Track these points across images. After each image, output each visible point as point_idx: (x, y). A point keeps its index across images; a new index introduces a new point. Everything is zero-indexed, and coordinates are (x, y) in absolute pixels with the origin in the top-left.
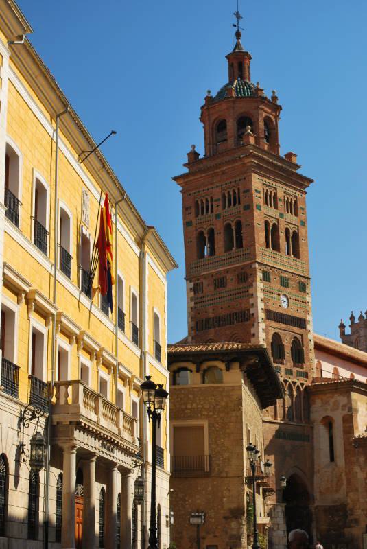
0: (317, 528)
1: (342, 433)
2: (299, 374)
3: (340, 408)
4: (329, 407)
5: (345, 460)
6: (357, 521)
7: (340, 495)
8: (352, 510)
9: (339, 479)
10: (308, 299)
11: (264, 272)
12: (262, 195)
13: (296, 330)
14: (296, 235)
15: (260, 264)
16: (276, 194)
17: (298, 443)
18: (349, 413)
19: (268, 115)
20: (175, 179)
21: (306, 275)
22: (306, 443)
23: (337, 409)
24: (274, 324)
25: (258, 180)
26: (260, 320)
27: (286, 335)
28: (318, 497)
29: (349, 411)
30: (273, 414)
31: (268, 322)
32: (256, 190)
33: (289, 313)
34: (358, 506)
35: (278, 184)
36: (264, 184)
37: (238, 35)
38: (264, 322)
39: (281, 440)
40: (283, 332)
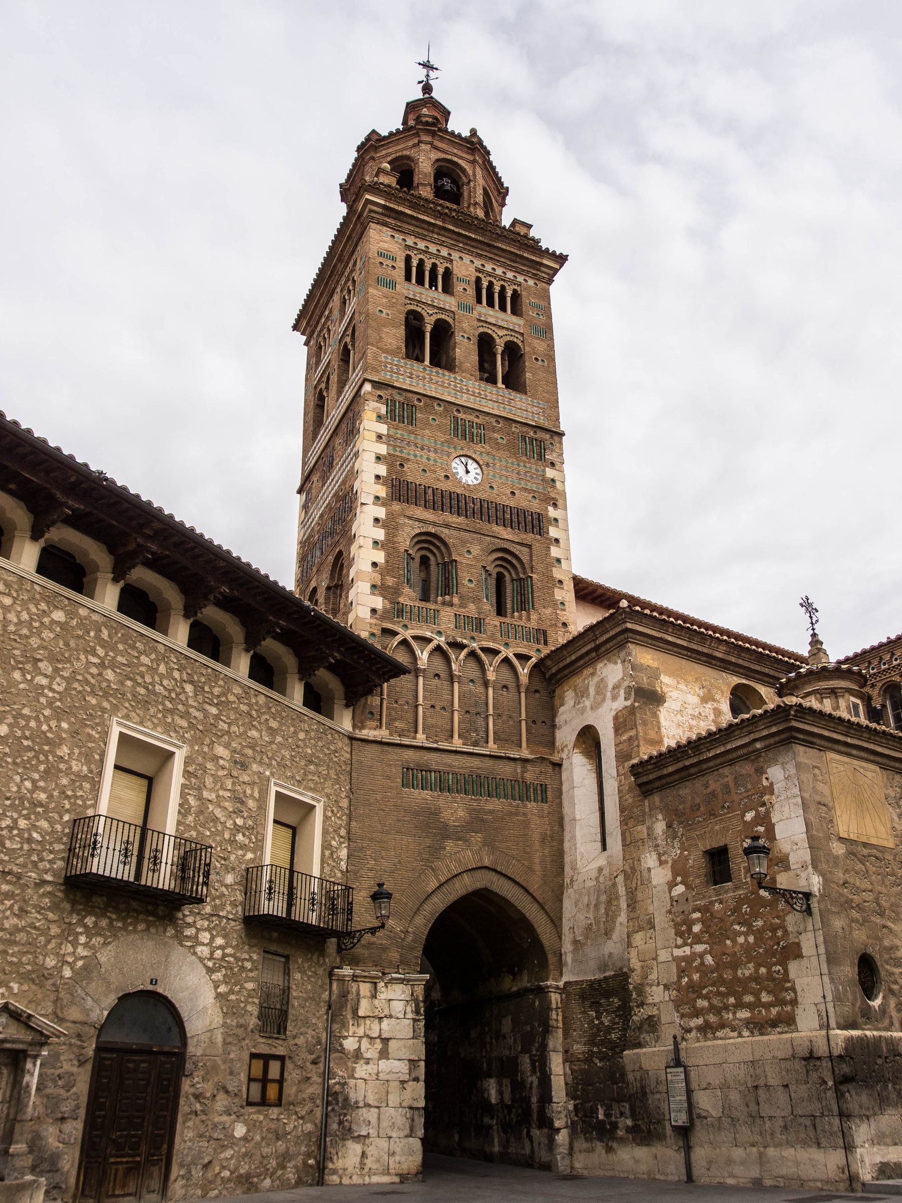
0: (566, 1051)
1: (614, 763)
2: (506, 632)
3: (609, 695)
4: (588, 703)
5: (624, 840)
6: (652, 1024)
7: (612, 946)
8: (640, 989)
9: (613, 897)
11: (391, 404)
12: (401, 265)
13: (505, 533)
14: (513, 352)
15: (377, 385)
16: (448, 273)
17: (494, 804)
18: (628, 703)
19: (449, 157)
20: (295, 328)
21: (546, 424)
22: (531, 805)
23: (604, 700)
24: (419, 512)
25: (389, 239)
26: (366, 497)
27: (464, 542)
28: (568, 959)
29: (626, 699)
31: (396, 507)
32: (380, 254)
33: (484, 496)
34: (653, 976)
35: (455, 255)
36: (408, 247)
37: (427, 88)
38: (383, 505)
39: (427, 794)
40: (452, 532)
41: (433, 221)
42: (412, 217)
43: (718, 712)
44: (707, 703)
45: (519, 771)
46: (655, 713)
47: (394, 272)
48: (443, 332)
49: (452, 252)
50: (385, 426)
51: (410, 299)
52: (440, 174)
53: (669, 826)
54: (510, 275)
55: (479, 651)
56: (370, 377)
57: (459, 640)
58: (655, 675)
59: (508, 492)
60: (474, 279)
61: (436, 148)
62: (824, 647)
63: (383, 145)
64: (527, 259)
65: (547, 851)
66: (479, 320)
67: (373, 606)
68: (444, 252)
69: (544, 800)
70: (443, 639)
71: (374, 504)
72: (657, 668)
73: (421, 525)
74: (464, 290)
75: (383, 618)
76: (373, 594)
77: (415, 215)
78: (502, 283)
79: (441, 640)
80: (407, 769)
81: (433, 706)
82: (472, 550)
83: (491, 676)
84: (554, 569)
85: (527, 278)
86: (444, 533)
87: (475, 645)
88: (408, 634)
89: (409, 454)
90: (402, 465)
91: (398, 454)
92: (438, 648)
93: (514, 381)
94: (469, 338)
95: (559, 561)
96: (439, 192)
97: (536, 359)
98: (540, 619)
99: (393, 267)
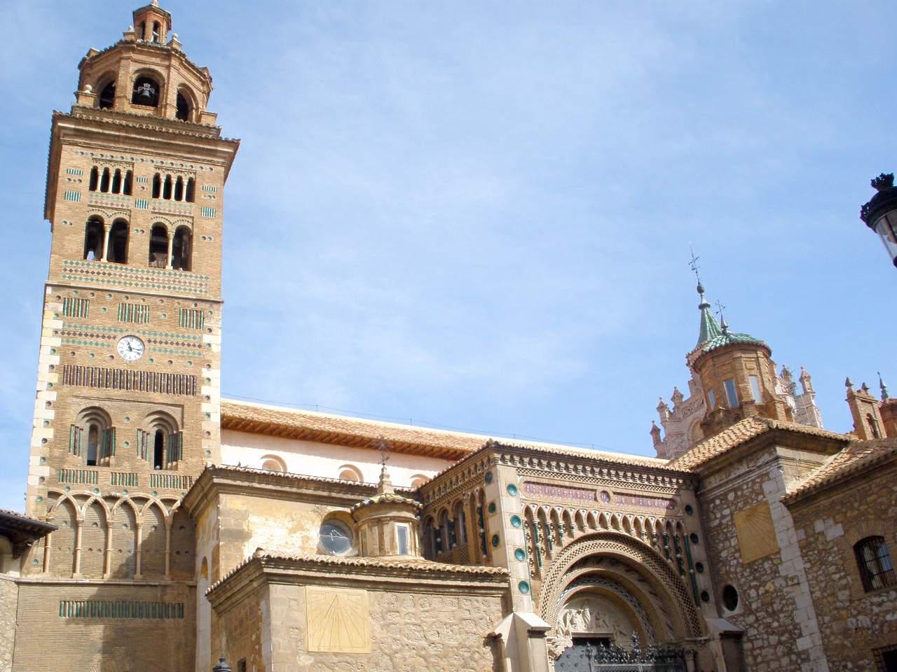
10: (207, 338)
11: (67, 303)
12: (87, 178)
15: (56, 287)
16: (130, 174)
18: (217, 542)
19: (147, 66)
22: (169, 622)
24: (85, 391)
27: (123, 411)
30: (67, 567)
31: (66, 389)
33: (143, 368)
35: (138, 157)
36: (96, 160)
38: (55, 389)
40: (114, 403)
41: (117, 134)
42: (99, 133)
43: (306, 539)
44: (295, 533)
45: (159, 595)
46: (240, 548)
47: (81, 185)
48: (121, 228)
49: (134, 156)
50: (61, 322)
51: (92, 206)
52: (139, 82)
53: (227, 641)
54: (188, 165)
55: (131, 502)
56: (50, 283)
57: (113, 494)
58: (244, 516)
59: (166, 361)
60: (152, 177)
61: (135, 61)
62: (390, 479)
63: (96, 62)
64: (203, 149)
65: (181, 656)
66: (153, 213)
67: (41, 475)
68: (128, 157)
69: (182, 616)
70: (99, 494)
71: (47, 390)
72: (246, 511)
73: (88, 401)
74: (142, 187)
75: (49, 483)
76: (41, 465)
77: (101, 131)
78: (179, 174)
79: (98, 496)
80: (65, 602)
81: (91, 549)
82: (129, 416)
83: (139, 521)
84: (203, 423)
85: (202, 165)
86: (106, 405)
87: (127, 496)
88: (69, 494)
89: (80, 343)
90: (74, 353)
91: (71, 344)
92: (96, 503)
93: (183, 262)
94: (143, 232)
95: (208, 415)
96: (138, 99)
97: (204, 238)
98: (186, 467)
99: (80, 181)
